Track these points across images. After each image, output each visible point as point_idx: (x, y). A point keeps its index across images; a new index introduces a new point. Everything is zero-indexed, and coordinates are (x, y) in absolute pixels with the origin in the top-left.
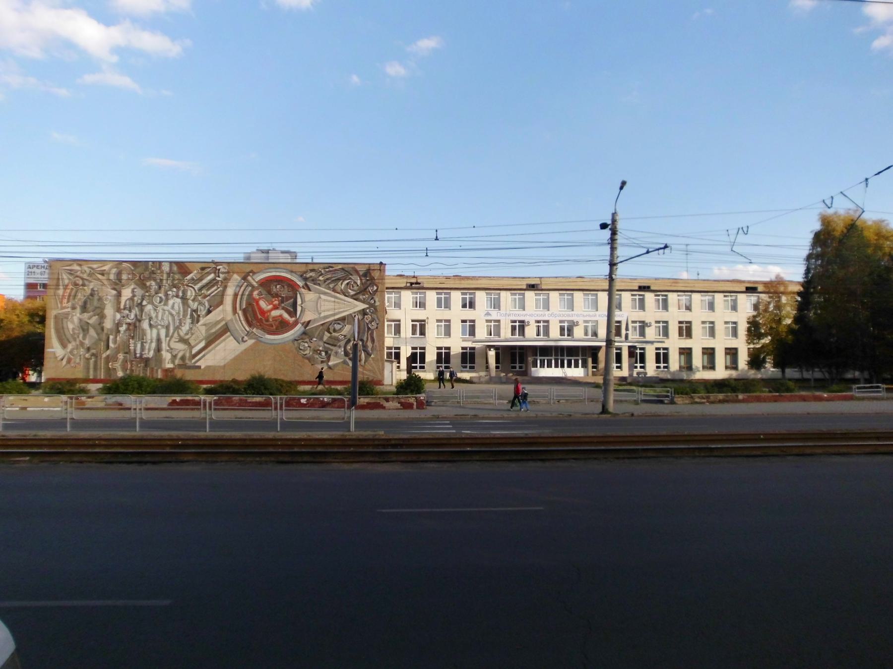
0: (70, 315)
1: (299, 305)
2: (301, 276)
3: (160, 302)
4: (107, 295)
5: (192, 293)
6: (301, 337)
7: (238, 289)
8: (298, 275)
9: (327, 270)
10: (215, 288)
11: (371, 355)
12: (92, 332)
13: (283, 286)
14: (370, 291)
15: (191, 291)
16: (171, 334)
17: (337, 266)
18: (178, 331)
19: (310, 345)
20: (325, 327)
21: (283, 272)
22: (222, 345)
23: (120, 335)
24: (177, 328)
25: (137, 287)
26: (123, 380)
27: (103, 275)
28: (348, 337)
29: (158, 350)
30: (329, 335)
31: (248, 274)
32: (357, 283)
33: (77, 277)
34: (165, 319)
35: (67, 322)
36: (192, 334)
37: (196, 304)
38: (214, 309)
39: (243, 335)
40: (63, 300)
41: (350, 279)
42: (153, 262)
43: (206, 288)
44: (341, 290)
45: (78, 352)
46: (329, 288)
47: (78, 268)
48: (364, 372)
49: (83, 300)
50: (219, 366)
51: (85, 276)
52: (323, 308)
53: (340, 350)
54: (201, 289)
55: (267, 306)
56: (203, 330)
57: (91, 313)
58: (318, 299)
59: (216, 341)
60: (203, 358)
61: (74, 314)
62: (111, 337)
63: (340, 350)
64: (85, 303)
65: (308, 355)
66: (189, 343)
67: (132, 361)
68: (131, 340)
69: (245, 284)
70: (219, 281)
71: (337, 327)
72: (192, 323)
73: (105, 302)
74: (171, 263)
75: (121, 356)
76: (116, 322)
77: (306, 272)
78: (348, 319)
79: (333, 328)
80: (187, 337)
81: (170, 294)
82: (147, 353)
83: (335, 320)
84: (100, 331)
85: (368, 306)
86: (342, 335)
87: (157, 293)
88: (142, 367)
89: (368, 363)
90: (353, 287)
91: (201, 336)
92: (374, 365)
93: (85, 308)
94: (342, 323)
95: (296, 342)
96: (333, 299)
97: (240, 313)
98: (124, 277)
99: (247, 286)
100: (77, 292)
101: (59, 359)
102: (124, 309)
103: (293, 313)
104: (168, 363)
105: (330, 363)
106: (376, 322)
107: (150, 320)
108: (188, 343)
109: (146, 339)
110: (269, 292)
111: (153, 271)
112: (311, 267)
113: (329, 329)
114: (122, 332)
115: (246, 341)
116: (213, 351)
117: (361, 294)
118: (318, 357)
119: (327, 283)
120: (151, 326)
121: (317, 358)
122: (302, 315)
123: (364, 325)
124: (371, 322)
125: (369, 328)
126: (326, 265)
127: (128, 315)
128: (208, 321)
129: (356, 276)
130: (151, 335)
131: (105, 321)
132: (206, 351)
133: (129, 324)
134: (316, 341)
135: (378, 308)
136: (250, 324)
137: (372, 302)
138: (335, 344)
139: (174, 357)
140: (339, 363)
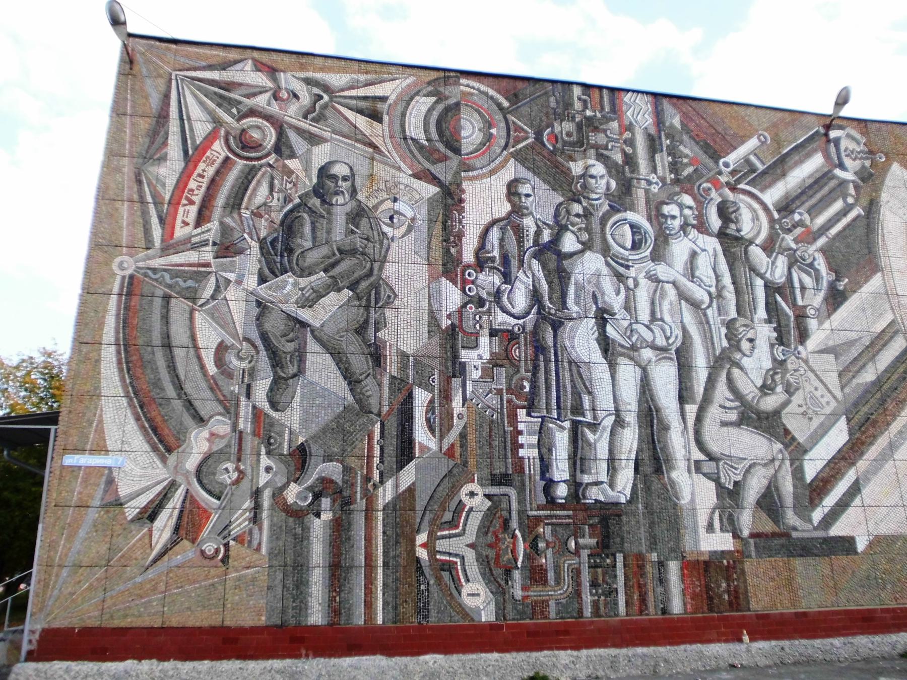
0: (213, 280)
3: (636, 246)
4: (395, 200)
5: (755, 218)
10: (838, 205)
15: (754, 211)
16: (699, 389)
18: (729, 374)
25: (529, 175)
26: (491, 626)
27: (375, 116)
34: (667, 318)
35: (192, 312)
36: (790, 390)
37: (782, 262)
38: (855, 287)
40: (181, 210)
45: (242, 473)
47: (260, 79)
49: (278, 217)
51: (291, 113)
54: (786, 207)
56: (829, 368)
57: (321, 276)
60: (857, 501)
61: (232, 276)
62: (421, 397)
64: (289, 226)
66: (787, 432)
67: (538, 519)
68: (522, 414)
73: (386, 229)
76: (445, 323)
80: (769, 403)
81: (674, 217)
82: (603, 477)
84: (359, 363)
88: (585, 553)
91: (829, 396)
93: (291, 251)
100: (248, 177)
101: (131, 511)
102: (481, 263)
104: (710, 528)
107: (605, 321)
108: (782, 432)
111: (589, 119)
120: (606, 345)
127: (498, 294)
132: (862, 465)
133: (509, 337)
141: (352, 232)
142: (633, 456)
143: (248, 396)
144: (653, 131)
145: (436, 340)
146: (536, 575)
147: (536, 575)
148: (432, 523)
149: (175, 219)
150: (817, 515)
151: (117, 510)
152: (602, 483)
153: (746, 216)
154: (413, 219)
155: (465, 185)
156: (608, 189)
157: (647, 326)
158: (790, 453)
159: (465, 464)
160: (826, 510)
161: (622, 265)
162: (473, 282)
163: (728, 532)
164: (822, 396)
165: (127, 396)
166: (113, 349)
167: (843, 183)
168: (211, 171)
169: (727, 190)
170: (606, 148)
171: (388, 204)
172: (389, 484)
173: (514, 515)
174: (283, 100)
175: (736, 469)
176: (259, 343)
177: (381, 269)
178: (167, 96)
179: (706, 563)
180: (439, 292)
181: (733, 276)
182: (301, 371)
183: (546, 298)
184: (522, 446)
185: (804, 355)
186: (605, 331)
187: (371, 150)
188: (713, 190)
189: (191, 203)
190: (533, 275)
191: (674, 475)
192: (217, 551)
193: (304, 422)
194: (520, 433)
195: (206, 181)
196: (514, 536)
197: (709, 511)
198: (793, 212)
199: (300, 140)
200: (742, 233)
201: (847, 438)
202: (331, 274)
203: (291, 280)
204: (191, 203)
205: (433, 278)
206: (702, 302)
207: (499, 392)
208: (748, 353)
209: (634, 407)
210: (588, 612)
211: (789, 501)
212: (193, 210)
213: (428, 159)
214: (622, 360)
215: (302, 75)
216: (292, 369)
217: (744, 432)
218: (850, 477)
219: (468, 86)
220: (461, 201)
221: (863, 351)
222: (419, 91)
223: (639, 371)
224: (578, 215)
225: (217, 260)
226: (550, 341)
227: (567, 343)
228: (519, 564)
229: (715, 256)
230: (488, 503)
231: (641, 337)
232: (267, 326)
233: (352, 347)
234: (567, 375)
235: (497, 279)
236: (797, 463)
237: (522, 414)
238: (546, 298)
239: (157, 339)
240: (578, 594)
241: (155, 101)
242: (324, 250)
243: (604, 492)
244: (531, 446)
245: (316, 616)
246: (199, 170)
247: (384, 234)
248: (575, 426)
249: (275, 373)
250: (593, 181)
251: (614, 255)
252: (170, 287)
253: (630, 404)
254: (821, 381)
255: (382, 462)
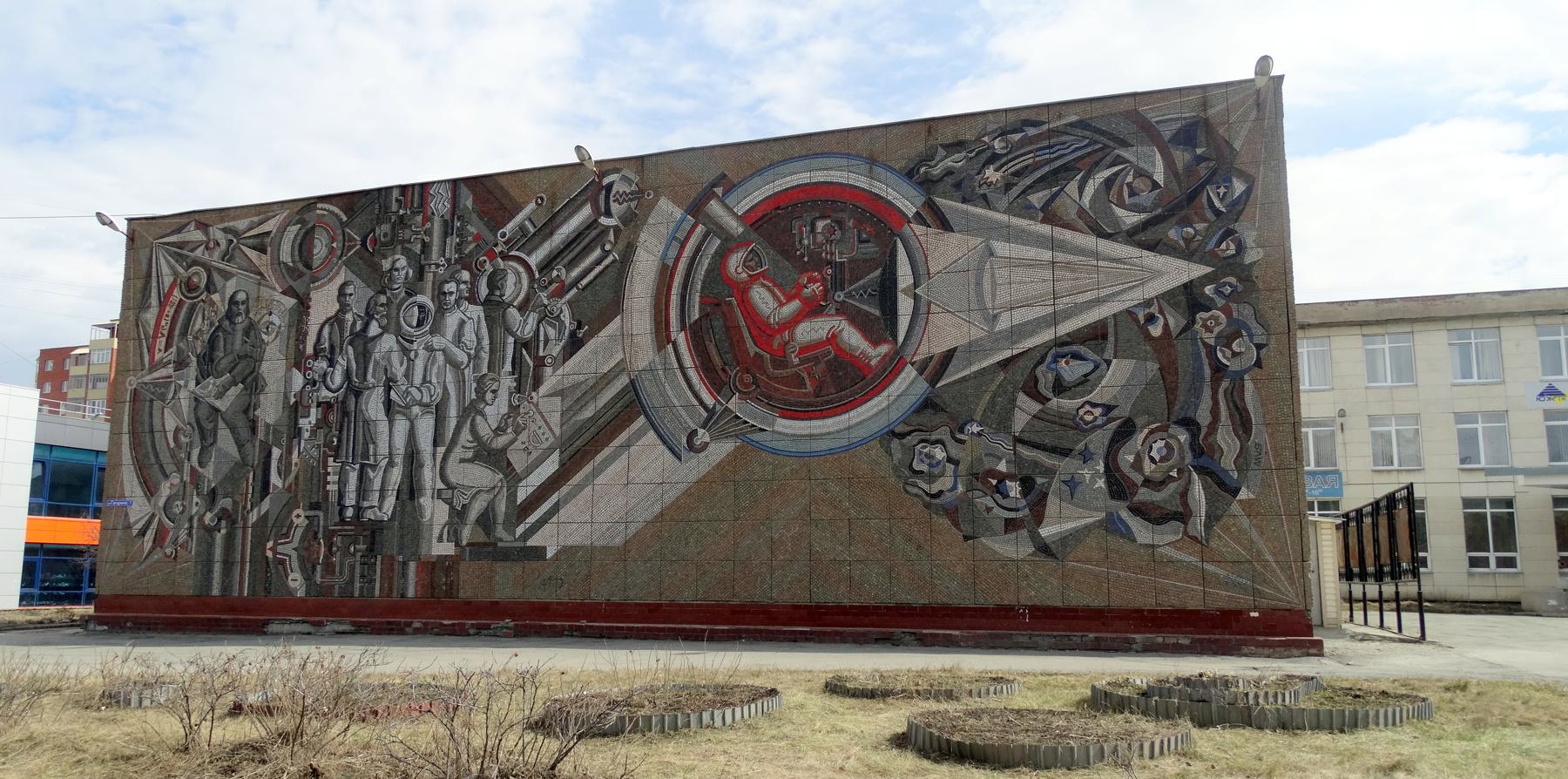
1: (904, 291)
2: (910, 174)
3: (420, 324)
4: (271, 314)
5: (519, 281)
6: (916, 420)
7: (673, 253)
8: (898, 172)
9: (1017, 137)
10: (597, 253)
11: (1235, 492)
12: (225, 440)
13: (840, 223)
14: (1217, 203)
15: (518, 274)
16: (449, 434)
17: (1060, 117)
18: (473, 420)
19: (955, 451)
20: (1019, 374)
21: (839, 168)
22: (618, 466)
23: (303, 442)
24: (470, 411)
26: (302, 600)
27: (262, 249)
28: (1124, 411)
29: (411, 490)
30: (1035, 407)
31: (707, 195)
32: (1150, 177)
33: (195, 262)
34: (434, 380)
36: (518, 431)
37: (532, 318)
38: (592, 334)
39: (693, 426)
41: (1118, 160)
42: (404, 189)
43: (566, 261)
44: (1081, 212)
46: (1027, 211)
48: (1209, 567)
49: (206, 337)
50: (606, 548)
51: (215, 258)
52: (1003, 297)
53: (1086, 473)
54: (546, 266)
55: (781, 305)
56: (553, 409)
58: (982, 263)
59: (597, 452)
60: (555, 519)
61: (182, 383)
62: (276, 452)
63: (1086, 473)
64: (212, 344)
65: (948, 498)
66: (509, 464)
67: (334, 533)
68: (331, 460)
69: (700, 229)
70: (608, 228)
71: (1071, 371)
72: (519, 389)
73: (264, 337)
74: (455, 183)
75: (299, 518)
76: (293, 400)
77: (927, 158)
78: (1116, 333)
79: (1050, 376)
80: (501, 441)
81: (451, 293)
83: (1059, 343)
84: (244, 433)
85: (1209, 270)
86: (1094, 405)
87: (410, 294)
88: (358, 558)
89: (1227, 529)
90: (1132, 194)
92: (1254, 534)
93: (212, 360)
94: (1091, 355)
95: (896, 441)
96: (1047, 255)
97: (681, 339)
98: (320, 249)
99: (705, 236)
100: (192, 309)
101: (135, 532)
102: (316, 356)
103: (881, 324)
104: (440, 539)
105: (1044, 532)
106: (1251, 336)
107: (390, 388)
109: (375, 455)
110: (786, 250)
112: (947, 135)
113: (1036, 381)
114: (306, 435)
115: (707, 444)
116: (588, 490)
117: (1174, 220)
118: (991, 504)
119: (1015, 191)
120: (389, 405)
121: (989, 510)
122: (918, 329)
123: (1197, 357)
124: (1227, 339)
125: (1219, 369)
126: (1012, 118)
127: (325, 375)
128: (568, 382)
129: (1145, 149)
130: (389, 438)
131: (262, 397)
132: (565, 490)
133: (326, 406)
134: (979, 434)
135: (1255, 272)
136: (717, 383)
137: (1229, 248)
138: (1068, 446)
139: (458, 515)
140: (1087, 529)
141: (246, 342)
142: (396, 488)
143: (189, 460)
144: (447, 217)
145: (286, 412)
146: (329, 568)
147: (329, 568)
148: (276, 535)
149: (155, 347)
150: (520, 530)
151: (129, 531)
152: (374, 507)
153: (511, 279)
154: (280, 327)
155: (313, 295)
156: (406, 279)
157: (418, 388)
158: (507, 482)
159: (296, 496)
160: (527, 526)
161: (407, 341)
162: (310, 369)
163: (452, 542)
164: (543, 434)
165: (134, 464)
166: (127, 436)
167: (607, 229)
168: (172, 310)
169: (499, 259)
170: (409, 242)
171: (266, 318)
172: (255, 511)
173: (321, 529)
174: (211, 249)
175: (466, 495)
176: (195, 425)
177: (260, 365)
178: (150, 260)
179: (433, 564)
180: (291, 379)
181: (491, 338)
182: (215, 441)
183: (354, 374)
184: (329, 483)
185: (535, 400)
186: (389, 396)
187: (259, 277)
188: (488, 262)
189: (163, 335)
190: (348, 358)
191: (422, 500)
192: (172, 552)
193: (215, 473)
194: (329, 474)
195: (169, 318)
196: (319, 543)
197: (441, 527)
198: (553, 269)
199: (220, 278)
200: (504, 298)
201: (557, 467)
202: (233, 374)
203: (212, 381)
204: (163, 335)
205: (288, 369)
206: (462, 363)
207: (319, 445)
208: (490, 402)
209: (402, 451)
210: (357, 593)
211: (500, 519)
212: (164, 339)
213: (291, 277)
214: (398, 417)
215: (221, 226)
216: (210, 440)
217: (476, 466)
218: (554, 498)
219: (322, 209)
220: (309, 307)
221: (586, 392)
222: (291, 221)
223: (408, 423)
224: (382, 305)
225: (177, 372)
226: (352, 407)
227: (364, 408)
228: (320, 561)
229: (479, 322)
230: (307, 522)
231: (414, 399)
232: (199, 414)
233: (241, 422)
234: (361, 430)
235: (324, 364)
236: (513, 489)
237: (331, 460)
238: (354, 374)
239: (147, 428)
240: (351, 581)
241: (144, 267)
242: (230, 358)
243: (375, 513)
244: (334, 483)
245: (216, 592)
246: (166, 313)
247: (263, 340)
248: (363, 466)
249: (202, 443)
250: (396, 273)
251: (403, 333)
252: (153, 393)
253: (399, 449)
254: (546, 421)
255: (252, 497)
